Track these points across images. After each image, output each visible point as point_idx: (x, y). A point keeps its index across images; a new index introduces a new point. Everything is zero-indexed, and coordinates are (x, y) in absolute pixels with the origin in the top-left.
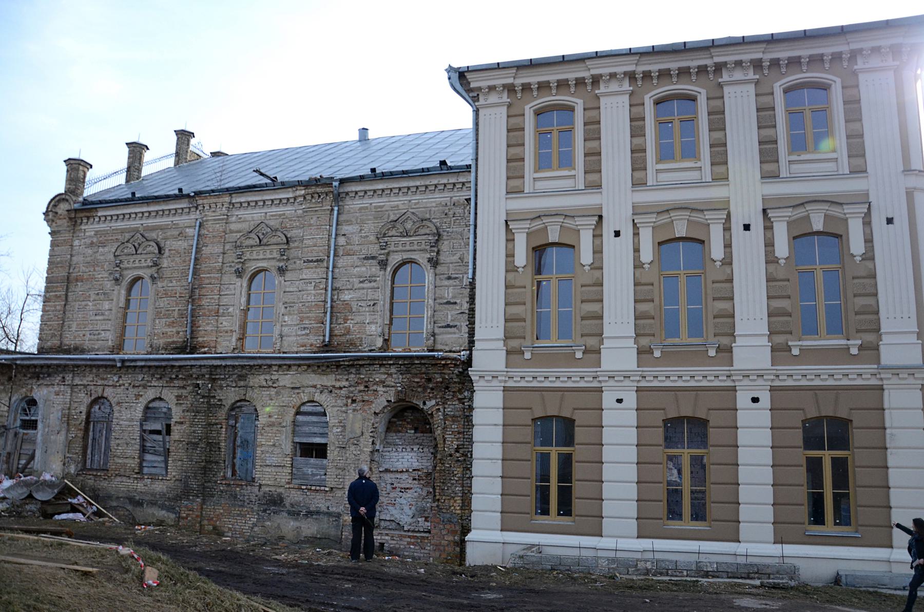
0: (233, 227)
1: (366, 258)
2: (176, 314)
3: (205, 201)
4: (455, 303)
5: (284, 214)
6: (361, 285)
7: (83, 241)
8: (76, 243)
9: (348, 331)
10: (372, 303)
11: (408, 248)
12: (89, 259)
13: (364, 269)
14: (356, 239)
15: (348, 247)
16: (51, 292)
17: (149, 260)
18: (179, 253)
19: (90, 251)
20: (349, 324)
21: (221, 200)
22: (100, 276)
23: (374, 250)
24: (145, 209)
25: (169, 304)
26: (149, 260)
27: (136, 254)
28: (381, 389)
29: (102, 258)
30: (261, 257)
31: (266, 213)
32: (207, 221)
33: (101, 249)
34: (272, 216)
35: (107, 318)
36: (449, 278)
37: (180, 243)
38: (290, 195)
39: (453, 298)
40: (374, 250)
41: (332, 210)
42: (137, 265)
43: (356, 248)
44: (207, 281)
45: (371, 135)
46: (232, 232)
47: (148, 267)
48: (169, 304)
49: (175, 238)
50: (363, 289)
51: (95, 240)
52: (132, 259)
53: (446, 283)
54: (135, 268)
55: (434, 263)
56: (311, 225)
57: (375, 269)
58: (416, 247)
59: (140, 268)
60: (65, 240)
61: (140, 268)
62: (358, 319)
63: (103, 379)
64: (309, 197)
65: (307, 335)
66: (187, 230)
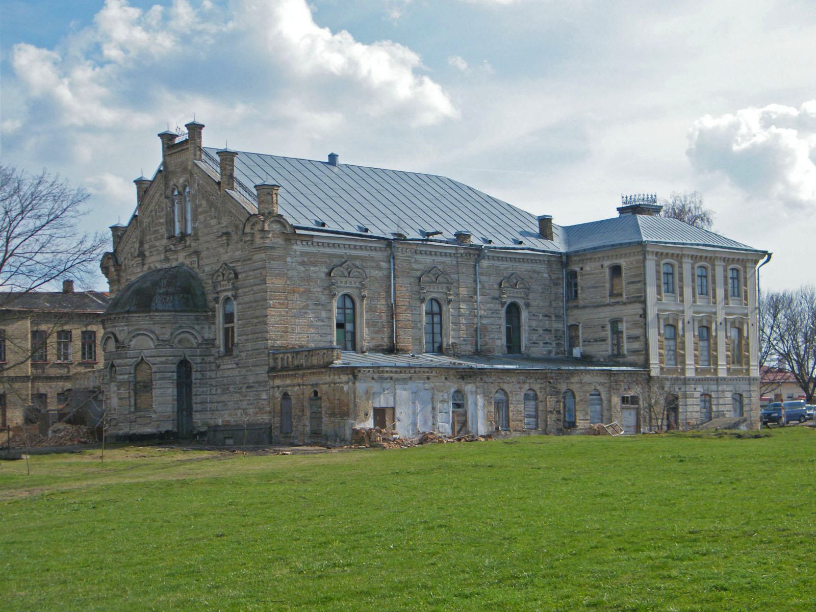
0: (415, 266)
1: (494, 298)
2: (379, 324)
3: (401, 246)
4: (537, 330)
5: (444, 262)
6: (493, 315)
7: (295, 259)
8: (289, 259)
9: (486, 344)
10: (498, 327)
11: (515, 295)
12: (302, 275)
13: (492, 305)
14: (486, 285)
15: (483, 290)
16: (274, 299)
17: (357, 283)
18: (377, 280)
19: (302, 269)
20: (487, 339)
21: (411, 247)
22: (314, 290)
23: (496, 294)
24: (353, 243)
25: (374, 317)
26: (357, 283)
27: (349, 277)
28: (622, 384)
29: (314, 275)
30: (436, 290)
31: (434, 260)
32: (398, 259)
33: (312, 268)
34: (437, 262)
35: (326, 324)
36: (534, 315)
37: (377, 272)
38: (453, 252)
39: (536, 327)
40: (496, 294)
41: (476, 265)
42: (348, 285)
43: (488, 291)
44: (403, 304)
45: (341, 161)
46: (413, 269)
47: (357, 287)
48: (374, 317)
49: (372, 268)
50: (492, 317)
51: (306, 260)
52: (344, 280)
53: (533, 318)
54: (347, 287)
55: (528, 305)
56: (463, 273)
57: (498, 307)
58: (519, 295)
59: (351, 287)
60: (280, 256)
61: (351, 287)
62: (492, 336)
63: (501, 379)
64: (464, 255)
65: (466, 344)
66: (381, 263)
